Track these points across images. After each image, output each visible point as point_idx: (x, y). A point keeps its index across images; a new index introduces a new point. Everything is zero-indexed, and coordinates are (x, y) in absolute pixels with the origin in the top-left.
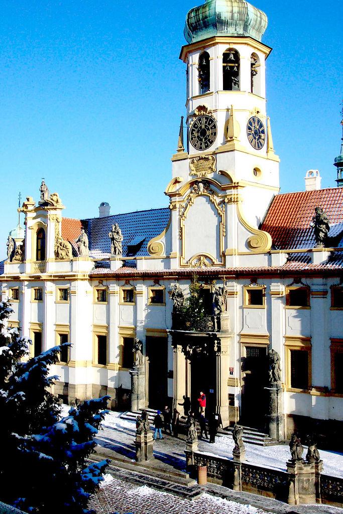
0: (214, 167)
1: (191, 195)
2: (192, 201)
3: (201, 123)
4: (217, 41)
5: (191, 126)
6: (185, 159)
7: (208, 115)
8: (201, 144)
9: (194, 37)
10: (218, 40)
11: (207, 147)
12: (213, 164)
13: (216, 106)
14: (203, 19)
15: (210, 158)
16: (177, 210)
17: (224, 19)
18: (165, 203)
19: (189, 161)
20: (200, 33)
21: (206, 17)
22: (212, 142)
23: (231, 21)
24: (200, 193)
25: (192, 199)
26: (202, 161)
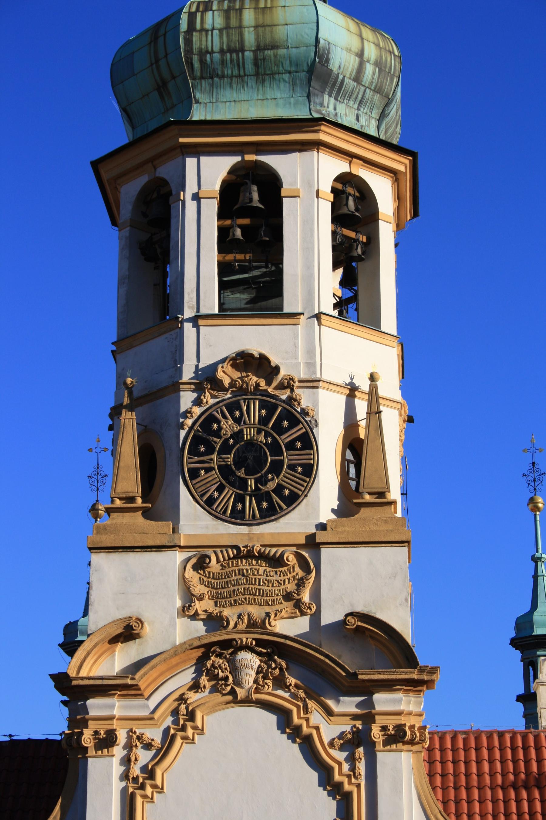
0: (306, 597)
1: (193, 697)
2: (199, 723)
3: (238, 421)
4: (322, 137)
5: (189, 422)
6: (159, 548)
7: (277, 393)
8: (240, 499)
9: (197, 102)
10: (326, 135)
11: (270, 513)
12: (300, 584)
13: (311, 365)
14: (259, 48)
15: (291, 559)
16: (118, 751)
17: (335, 70)
18: (48, 721)
19: (179, 557)
20: (227, 94)
21: (274, 47)
22: (293, 500)
23: (353, 84)
24: (241, 693)
25: (199, 715)
26: (244, 565)
